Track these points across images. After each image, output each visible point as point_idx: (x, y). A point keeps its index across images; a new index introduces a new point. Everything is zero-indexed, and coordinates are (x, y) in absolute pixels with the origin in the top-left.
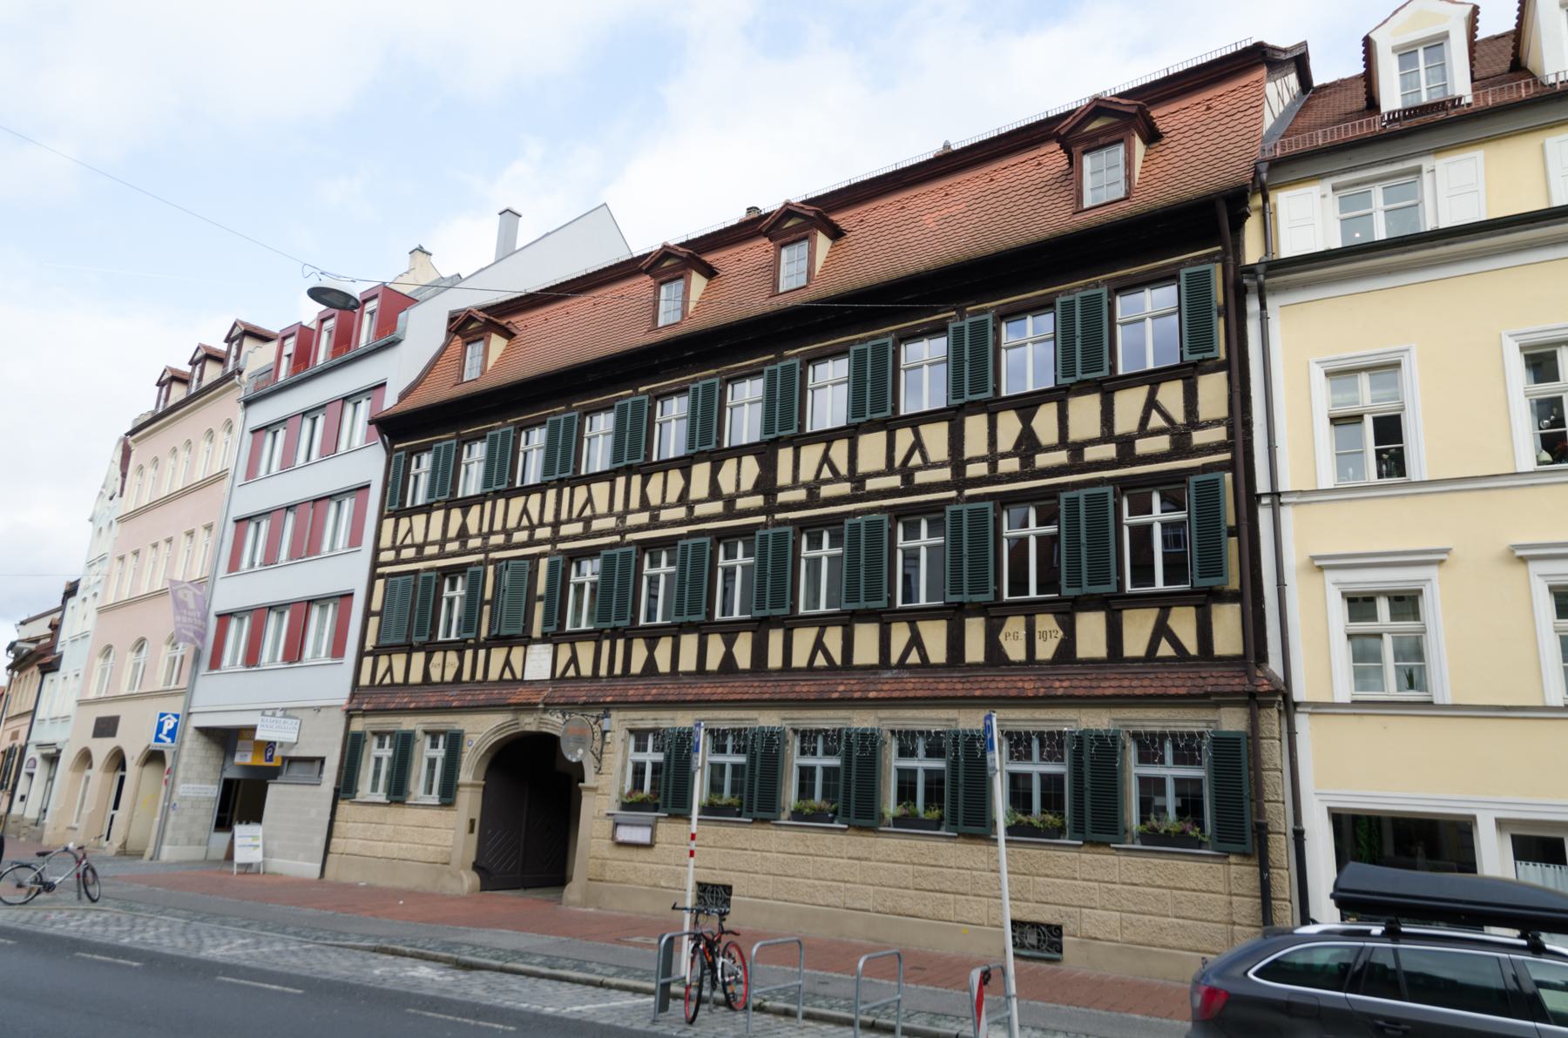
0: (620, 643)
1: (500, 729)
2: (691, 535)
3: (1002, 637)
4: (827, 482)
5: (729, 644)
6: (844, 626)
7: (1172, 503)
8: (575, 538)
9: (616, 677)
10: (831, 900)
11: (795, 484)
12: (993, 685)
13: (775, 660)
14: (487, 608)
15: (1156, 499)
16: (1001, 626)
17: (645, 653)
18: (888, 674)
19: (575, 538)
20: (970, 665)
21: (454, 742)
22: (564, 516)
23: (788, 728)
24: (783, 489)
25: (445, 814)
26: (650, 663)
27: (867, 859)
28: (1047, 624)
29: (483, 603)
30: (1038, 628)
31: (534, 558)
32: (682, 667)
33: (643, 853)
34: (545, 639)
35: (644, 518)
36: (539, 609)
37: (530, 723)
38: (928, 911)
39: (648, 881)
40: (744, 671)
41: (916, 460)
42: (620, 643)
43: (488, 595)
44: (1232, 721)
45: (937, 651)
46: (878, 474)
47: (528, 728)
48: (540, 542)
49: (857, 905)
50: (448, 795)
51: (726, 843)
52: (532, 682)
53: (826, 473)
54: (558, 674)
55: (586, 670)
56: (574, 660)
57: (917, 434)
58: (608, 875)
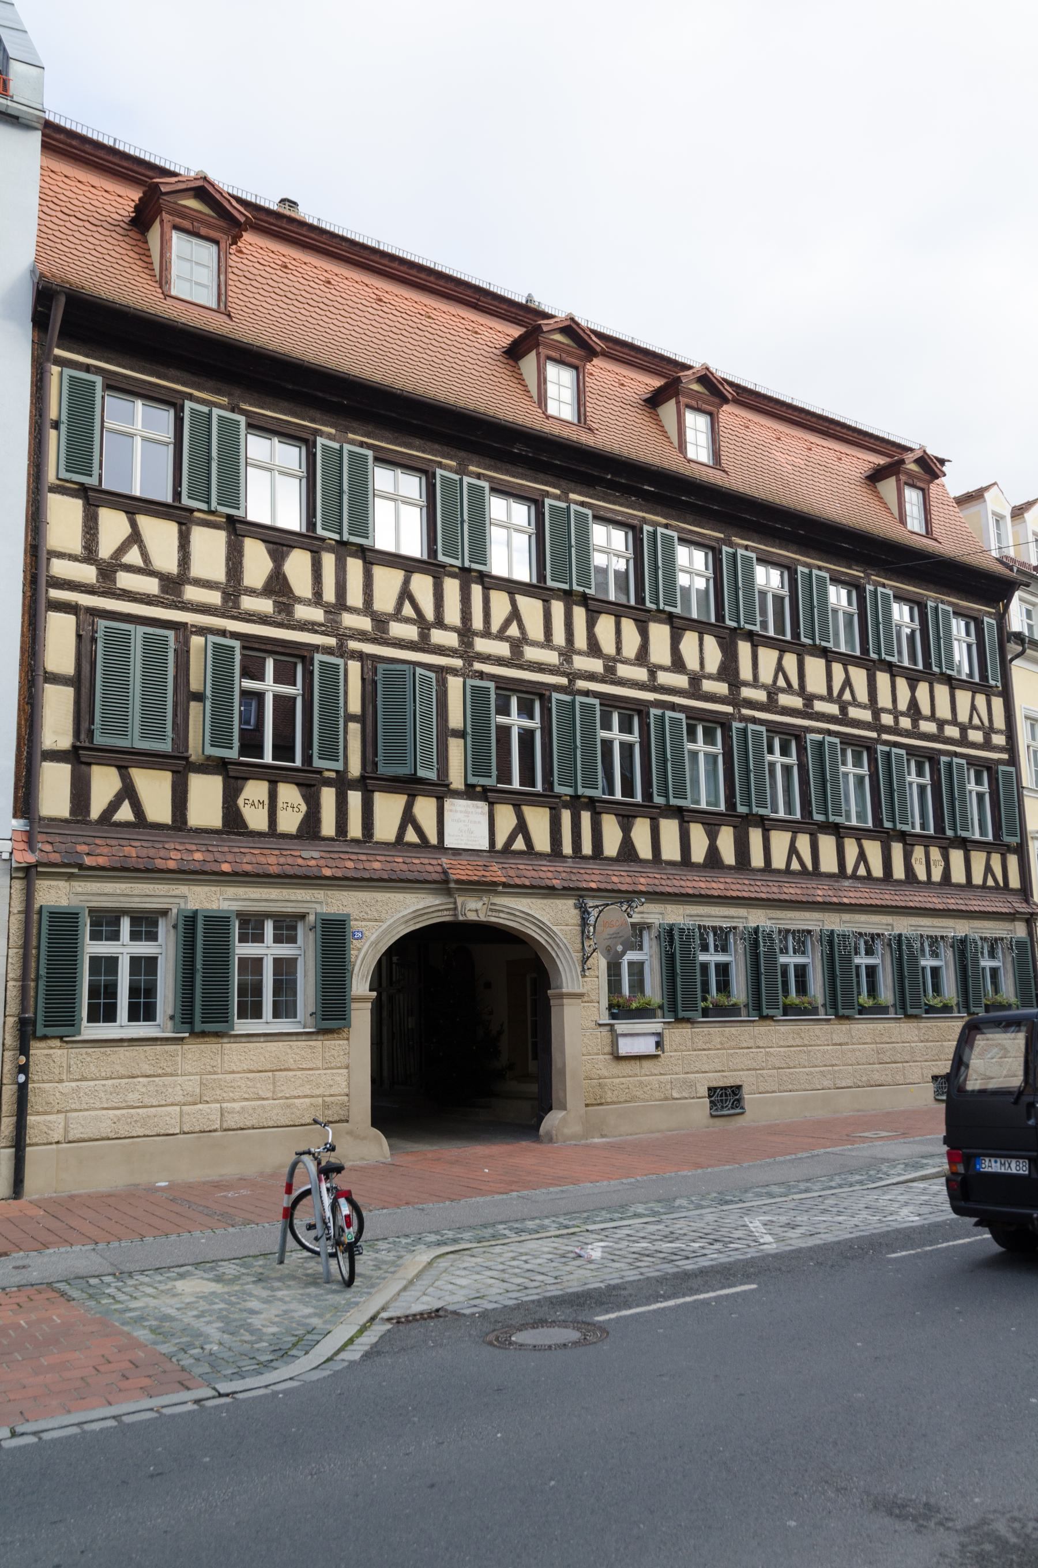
0: (586, 817)
1: (417, 915)
2: (658, 704)
3: (913, 861)
4: (782, 690)
5: (712, 837)
6: (811, 834)
7: (284, 676)
8: (500, 661)
9: (585, 858)
10: (826, 1083)
11: (755, 683)
12: (916, 899)
13: (757, 860)
14: (354, 728)
15: (270, 665)
16: (912, 852)
17: (619, 835)
18: (847, 883)
19: (500, 661)
20: (896, 881)
21: (334, 934)
22: (478, 624)
23: (977, 938)
24: (746, 684)
25: (334, 1046)
26: (713, 852)
27: (847, 1044)
28: (935, 853)
29: (361, 719)
30: (932, 858)
31: (442, 672)
32: (665, 856)
33: (647, 1064)
34: (470, 792)
35: (596, 665)
36: (456, 749)
37: (474, 909)
38: (889, 1079)
39: (657, 1095)
40: (730, 867)
41: (847, 696)
42: (586, 817)
43: (355, 706)
44: (1020, 931)
45: (158, 806)
46: (821, 698)
47: (472, 917)
48: (441, 650)
49: (844, 1084)
50: (332, 1015)
51: (733, 1044)
52: (457, 852)
53: (781, 683)
54: (499, 845)
55: (542, 842)
56: (522, 828)
57: (134, 525)
58: (609, 1096)
